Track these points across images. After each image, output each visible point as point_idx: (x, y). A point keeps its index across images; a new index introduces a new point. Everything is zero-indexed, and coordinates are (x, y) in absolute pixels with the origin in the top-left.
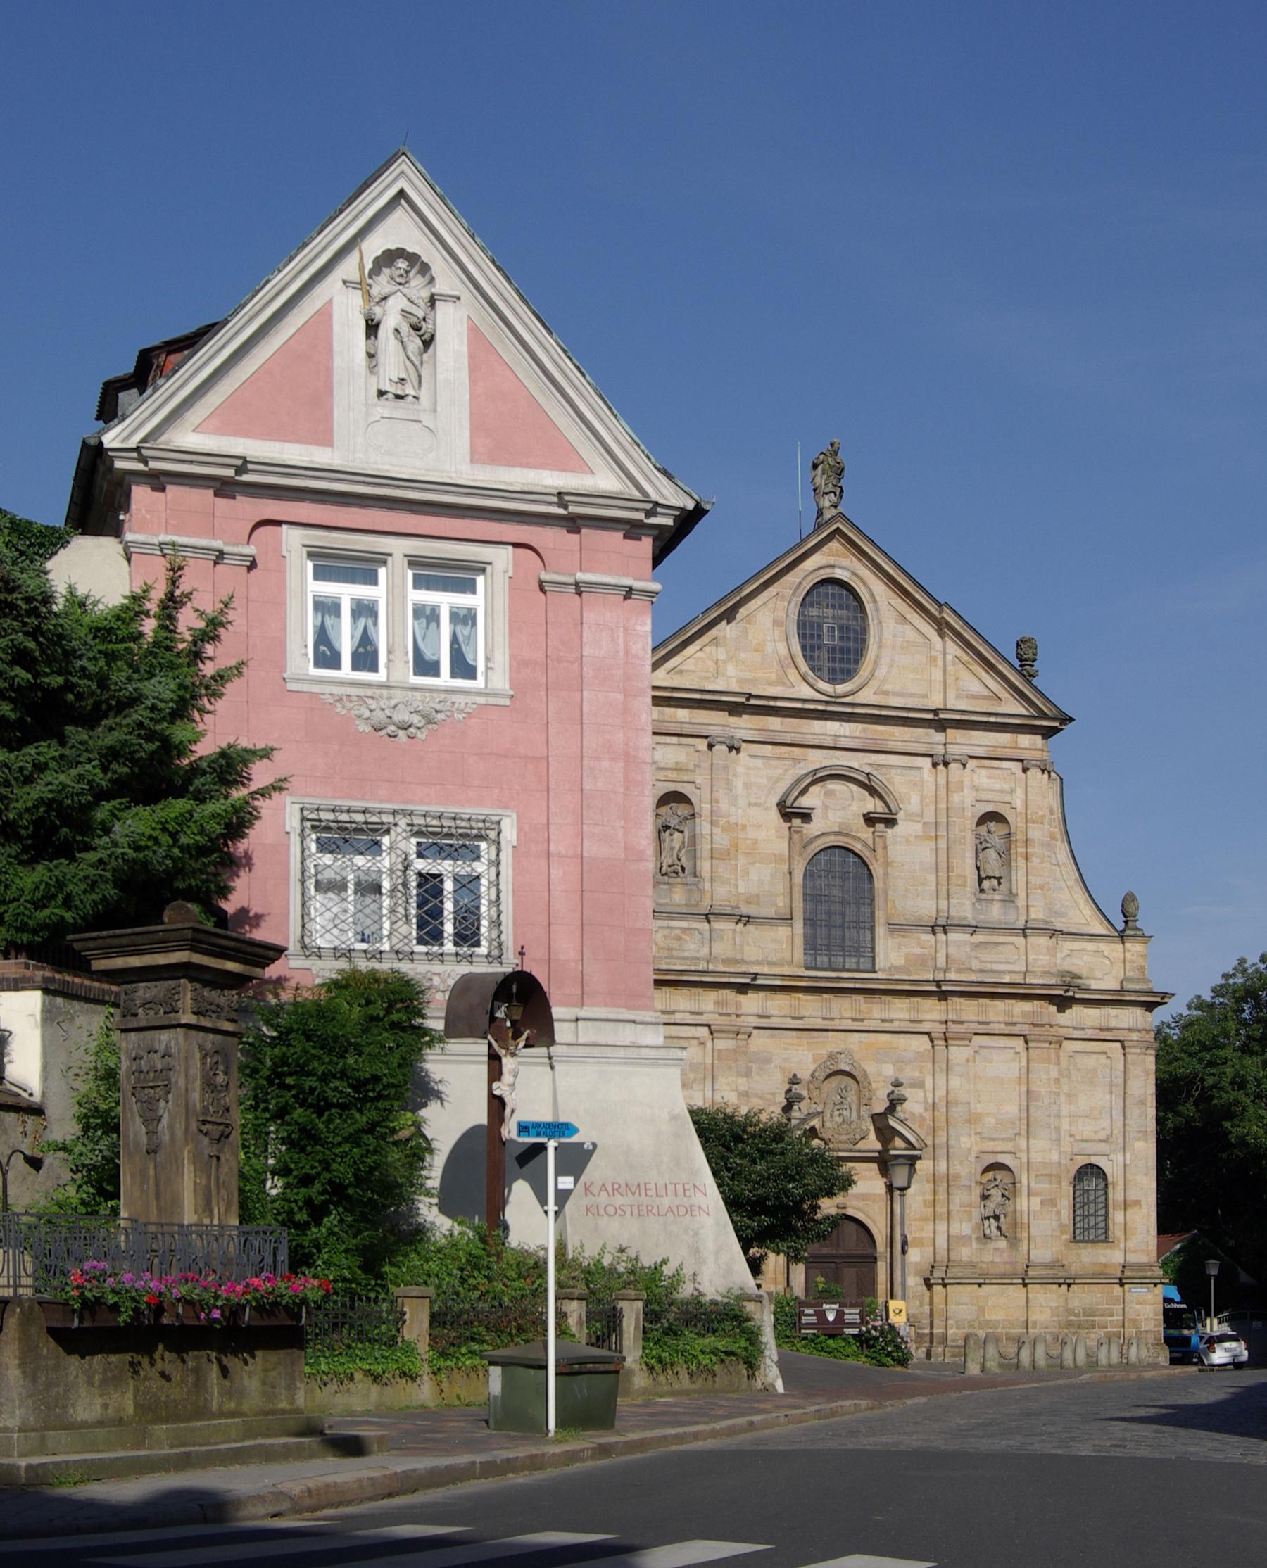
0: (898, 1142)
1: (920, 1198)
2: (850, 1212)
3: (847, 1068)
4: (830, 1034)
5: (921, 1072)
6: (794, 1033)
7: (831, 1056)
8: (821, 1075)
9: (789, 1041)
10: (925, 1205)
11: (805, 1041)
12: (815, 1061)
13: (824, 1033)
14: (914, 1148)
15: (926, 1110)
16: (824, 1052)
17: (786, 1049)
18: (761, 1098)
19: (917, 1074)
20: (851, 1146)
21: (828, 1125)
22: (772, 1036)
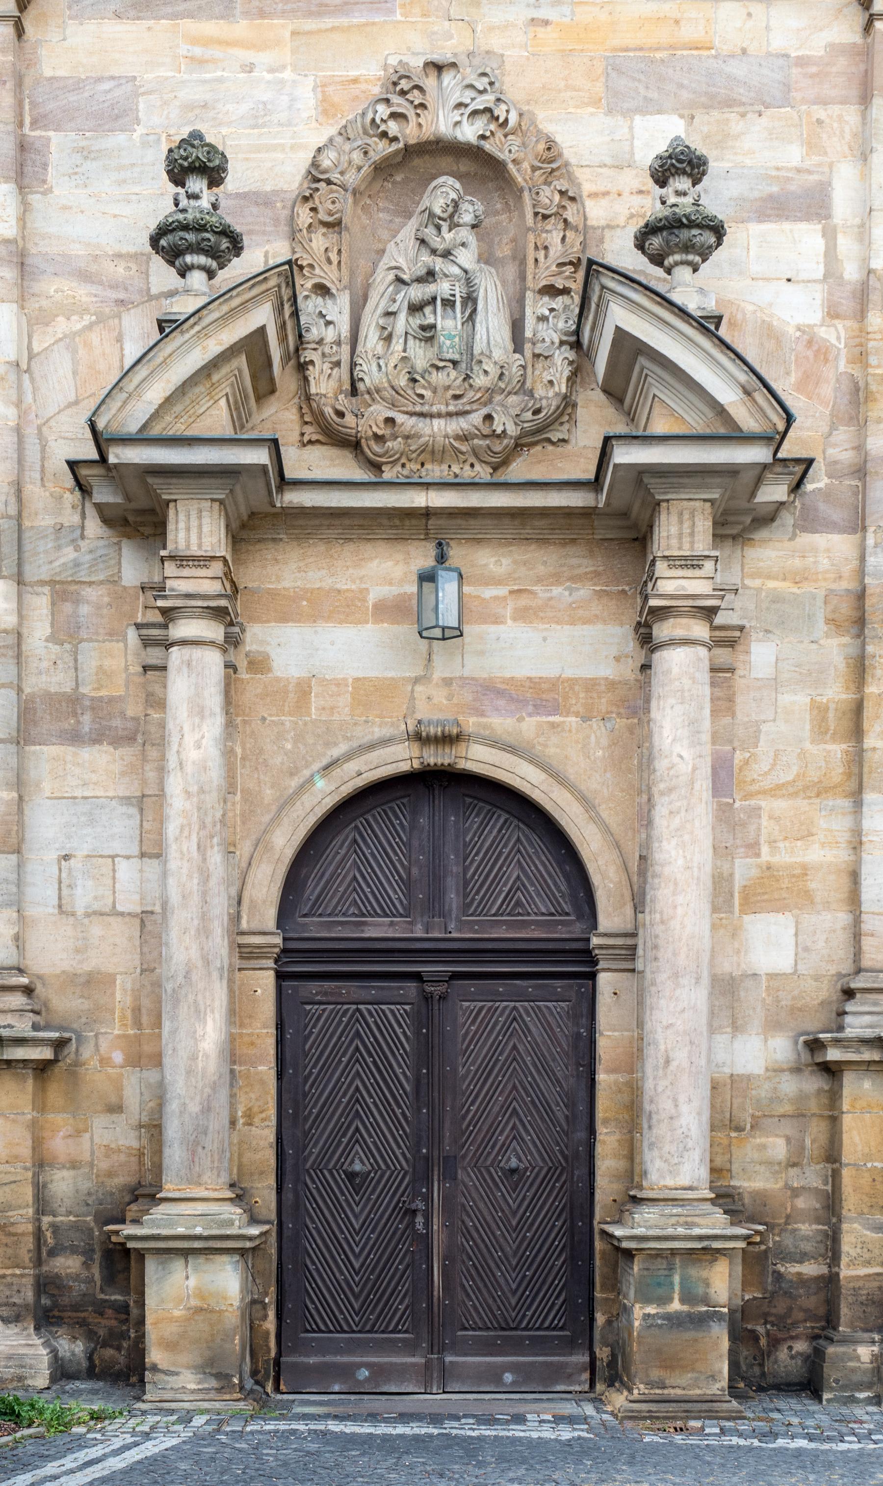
1: (797, 700)
2: (478, 758)
5: (812, 145)
8: (351, 165)
10: (821, 731)
12: (327, 108)
15: (832, 314)
16: (369, 70)
17: (200, 63)
19: (793, 155)
20: (482, 472)
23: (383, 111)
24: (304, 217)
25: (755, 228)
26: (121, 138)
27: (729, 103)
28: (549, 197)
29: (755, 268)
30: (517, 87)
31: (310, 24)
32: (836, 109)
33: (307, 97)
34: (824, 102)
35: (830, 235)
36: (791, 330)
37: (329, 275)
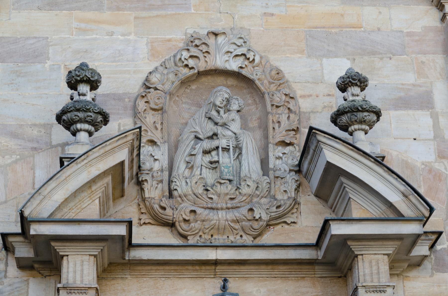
0: (360, 206)
12: (153, 53)
14: (400, 218)
16: (177, 35)
18: (14, 135)
19: (410, 78)
21: (181, 187)
23: (185, 54)
24: (141, 105)
26: (39, 66)
27: (373, 53)
28: (279, 98)
30: (258, 45)
31: (144, 14)
32: (431, 57)
33: (143, 48)
34: (425, 53)
35: (435, 117)
36: (419, 165)
37: (157, 136)
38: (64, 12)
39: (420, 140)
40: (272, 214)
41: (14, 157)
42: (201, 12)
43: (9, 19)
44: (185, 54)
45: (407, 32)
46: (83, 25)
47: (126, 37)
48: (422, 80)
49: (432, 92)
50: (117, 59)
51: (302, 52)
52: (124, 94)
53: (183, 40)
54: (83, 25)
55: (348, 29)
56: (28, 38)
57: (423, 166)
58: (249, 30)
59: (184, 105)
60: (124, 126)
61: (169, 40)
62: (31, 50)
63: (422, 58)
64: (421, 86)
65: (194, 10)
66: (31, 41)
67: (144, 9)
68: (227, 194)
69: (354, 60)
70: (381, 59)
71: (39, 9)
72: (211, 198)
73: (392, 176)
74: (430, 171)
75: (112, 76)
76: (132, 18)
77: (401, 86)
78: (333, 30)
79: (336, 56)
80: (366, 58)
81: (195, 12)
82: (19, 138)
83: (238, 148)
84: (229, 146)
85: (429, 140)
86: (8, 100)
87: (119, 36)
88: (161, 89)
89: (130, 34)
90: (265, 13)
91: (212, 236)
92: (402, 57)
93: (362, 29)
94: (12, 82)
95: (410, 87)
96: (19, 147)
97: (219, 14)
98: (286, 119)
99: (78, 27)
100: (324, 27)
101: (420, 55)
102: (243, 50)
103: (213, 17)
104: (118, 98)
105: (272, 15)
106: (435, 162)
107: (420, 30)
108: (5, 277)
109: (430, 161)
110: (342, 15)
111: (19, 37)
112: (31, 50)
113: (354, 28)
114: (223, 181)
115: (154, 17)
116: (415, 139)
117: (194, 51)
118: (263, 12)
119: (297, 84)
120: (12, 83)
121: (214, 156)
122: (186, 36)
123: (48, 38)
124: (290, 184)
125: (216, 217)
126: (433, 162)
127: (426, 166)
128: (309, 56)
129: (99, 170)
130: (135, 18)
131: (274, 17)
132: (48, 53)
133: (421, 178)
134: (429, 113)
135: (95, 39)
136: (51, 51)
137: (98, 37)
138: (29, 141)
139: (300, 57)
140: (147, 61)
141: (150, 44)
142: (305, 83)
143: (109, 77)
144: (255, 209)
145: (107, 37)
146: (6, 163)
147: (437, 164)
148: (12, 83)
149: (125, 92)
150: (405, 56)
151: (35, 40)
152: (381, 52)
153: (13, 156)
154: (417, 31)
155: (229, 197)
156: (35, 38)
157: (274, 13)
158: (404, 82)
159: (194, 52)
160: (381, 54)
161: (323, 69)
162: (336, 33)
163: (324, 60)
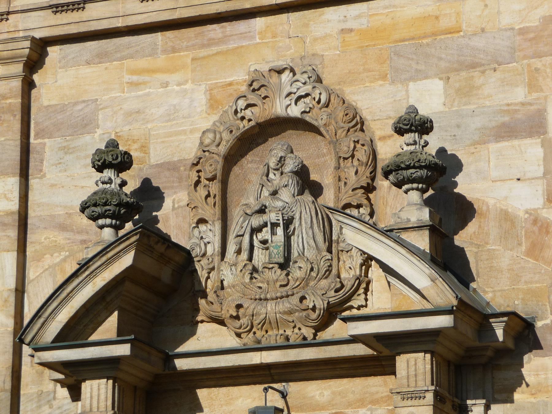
3: (295, 111)
4: (259, 22)
5: (533, 86)
6: (158, 37)
7: (257, 86)
9: (142, 63)
11: (186, 56)
12: (213, 103)
13: (242, 26)
16: (240, 77)
18: (63, 228)
19: (519, 94)
22: (102, 57)
25: (493, 147)
27: (473, 66)
29: (494, 174)
31: (203, 53)
33: (201, 98)
34: (539, 56)
36: (521, 214)
38: (114, 63)
39: (525, 180)
40: (330, 300)
41: (64, 254)
42: (268, 40)
43: (56, 82)
44: (242, 103)
45: (520, 29)
46: (135, 78)
47: (182, 86)
48: (535, 95)
49: (545, 111)
50: (172, 117)
51: (384, 77)
52: (180, 161)
53: (245, 81)
54: (135, 78)
55: (443, 37)
56: (76, 104)
57: (527, 216)
58: (322, 56)
59: (250, 165)
60: (178, 202)
61: (230, 84)
62: (79, 118)
63: (537, 63)
64: (530, 104)
65: (260, 39)
66: (79, 107)
67: (203, 46)
68: (277, 280)
69: (449, 78)
70: (483, 72)
71: (88, 63)
72: (260, 288)
73: (415, 258)
74: (535, 221)
75: (167, 139)
76: (189, 61)
77: (506, 108)
78: (425, 41)
79: (426, 78)
80: (464, 74)
81: (260, 41)
82: (68, 231)
83: (288, 223)
84: (278, 220)
85: (537, 178)
86: (56, 185)
87: (175, 87)
88: (215, 152)
89: (187, 81)
90: (342, 30)
91: (267, 332)
92: (511, 65)
93: (462, 33)
94: (60, 161)
95: (517, 108)
96: (68, 241)
97: (288, 40)
98: (354, 174)
99: (130, 81)
100: (413, 39)
101: (533, 60)
102: (308, 88)
103: (281, 44)
104: (171, 167)
105: (351, 30)
106: (543, 208)
107: (537, 23)
108: (54, 398)
109: (536, 207)
110: (437, 18)
111: (66, 103)
112: (79, 118)
113: (450, 33)
114: (271, 266)
115: (213, 55)
116: (519, 179)
117: (253, 98)
118: (340, 28)
119: (376, 122)
120: (60, 163)
121: (265, 234)
122: (249, 75)
123: (97, 100)
124: (355, 259)
125: (263, 311)
126: (539, 208)
127: (531, 214)
128: (393, 82)
129: (104, 280)
130: (193, 59)
131: (353, 34)
132: (98, 119)
133: (523, 233)
134: (540, 140)
135: (148, 94)
136: (100, 117)
137: (151, 90)
138: (78, 233)
139: (381, 85)
140: (205, 115)
141: (208, 92)
142: (387, 119)
143: (163, 142)
144: (307, 296)
145: (162, 89)
146: (55, 262)
147: (545, 210)
148: (60, 163)
149: (181, 158)
150: (515, 64)
151: (83, 105)
152: (483, 62)
153: (62, 253)
154: (533, 25)
155: (279, 284)
156: (84, 101)
157: (354, 27)
158: (510, 102)
159: (252, 99)
160: (483, 65)
161: (409, 97)
162: (428, 44)
163: (411, 84)
